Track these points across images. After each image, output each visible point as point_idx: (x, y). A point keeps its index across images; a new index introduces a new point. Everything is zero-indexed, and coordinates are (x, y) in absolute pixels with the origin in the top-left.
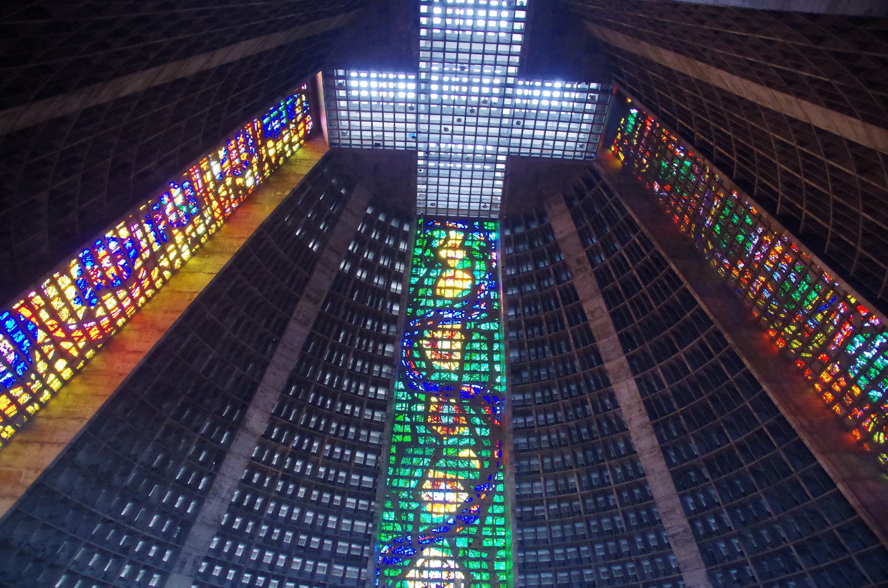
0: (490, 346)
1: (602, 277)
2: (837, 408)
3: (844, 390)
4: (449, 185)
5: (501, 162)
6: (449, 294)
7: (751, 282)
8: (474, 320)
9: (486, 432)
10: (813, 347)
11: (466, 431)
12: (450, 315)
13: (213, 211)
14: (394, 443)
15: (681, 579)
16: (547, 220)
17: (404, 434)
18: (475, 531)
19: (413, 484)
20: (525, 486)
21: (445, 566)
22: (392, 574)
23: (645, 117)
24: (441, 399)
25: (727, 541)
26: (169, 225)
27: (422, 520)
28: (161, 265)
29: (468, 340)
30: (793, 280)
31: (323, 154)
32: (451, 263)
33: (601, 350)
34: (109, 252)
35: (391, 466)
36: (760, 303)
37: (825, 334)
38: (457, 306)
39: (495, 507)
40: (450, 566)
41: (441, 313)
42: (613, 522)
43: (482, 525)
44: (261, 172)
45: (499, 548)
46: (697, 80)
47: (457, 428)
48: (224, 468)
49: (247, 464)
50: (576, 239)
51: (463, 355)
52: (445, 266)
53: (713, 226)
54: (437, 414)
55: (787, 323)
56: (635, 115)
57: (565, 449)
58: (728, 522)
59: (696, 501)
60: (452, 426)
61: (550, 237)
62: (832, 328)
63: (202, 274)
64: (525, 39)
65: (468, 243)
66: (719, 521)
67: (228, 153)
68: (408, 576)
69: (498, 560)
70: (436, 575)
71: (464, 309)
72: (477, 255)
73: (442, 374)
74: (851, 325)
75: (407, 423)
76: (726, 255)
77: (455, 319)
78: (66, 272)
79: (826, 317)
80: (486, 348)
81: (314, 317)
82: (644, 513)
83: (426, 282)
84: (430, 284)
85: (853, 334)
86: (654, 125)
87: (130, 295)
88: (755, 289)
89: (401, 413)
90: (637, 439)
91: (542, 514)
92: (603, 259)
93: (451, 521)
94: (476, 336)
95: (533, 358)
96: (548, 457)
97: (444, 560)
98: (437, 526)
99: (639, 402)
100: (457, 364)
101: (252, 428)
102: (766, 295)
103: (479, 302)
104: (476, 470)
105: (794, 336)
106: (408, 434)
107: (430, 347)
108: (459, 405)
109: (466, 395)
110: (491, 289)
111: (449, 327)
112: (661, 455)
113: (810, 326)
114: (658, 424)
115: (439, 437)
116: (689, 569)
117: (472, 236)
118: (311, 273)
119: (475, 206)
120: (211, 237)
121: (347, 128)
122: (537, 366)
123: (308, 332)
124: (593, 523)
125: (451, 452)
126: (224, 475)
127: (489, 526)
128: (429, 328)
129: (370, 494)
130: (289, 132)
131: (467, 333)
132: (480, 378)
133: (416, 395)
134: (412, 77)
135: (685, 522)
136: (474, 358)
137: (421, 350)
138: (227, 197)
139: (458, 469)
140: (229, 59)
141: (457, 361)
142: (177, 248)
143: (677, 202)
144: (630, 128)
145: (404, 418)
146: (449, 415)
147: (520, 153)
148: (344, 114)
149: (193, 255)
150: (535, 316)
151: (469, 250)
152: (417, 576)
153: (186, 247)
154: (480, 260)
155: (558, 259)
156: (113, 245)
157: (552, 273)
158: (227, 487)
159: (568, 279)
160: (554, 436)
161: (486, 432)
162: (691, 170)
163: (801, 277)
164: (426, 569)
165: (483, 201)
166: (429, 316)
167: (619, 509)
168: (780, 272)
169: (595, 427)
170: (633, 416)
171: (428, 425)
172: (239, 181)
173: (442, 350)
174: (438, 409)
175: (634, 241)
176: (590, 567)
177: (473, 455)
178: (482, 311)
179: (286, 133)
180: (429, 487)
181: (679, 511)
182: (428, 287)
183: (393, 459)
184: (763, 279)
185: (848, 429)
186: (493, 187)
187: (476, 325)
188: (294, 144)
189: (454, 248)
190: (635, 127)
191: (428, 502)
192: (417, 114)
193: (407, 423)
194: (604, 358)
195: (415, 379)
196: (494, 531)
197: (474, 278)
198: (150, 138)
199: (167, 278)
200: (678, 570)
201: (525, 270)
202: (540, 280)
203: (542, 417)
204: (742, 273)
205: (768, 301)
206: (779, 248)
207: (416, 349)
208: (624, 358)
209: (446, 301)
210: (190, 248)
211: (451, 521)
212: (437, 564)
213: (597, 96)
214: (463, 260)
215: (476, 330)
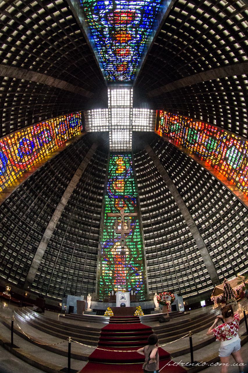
3: (228, 169)
6: (120, 172)
7: (199, 149)
9: (132, 208)
11: (127, 209)
12: (120, 177)
19: (112, 224)
26: (43, 141)
28: (40, 152)
29: (126, 183)
30: (210, 143)
32: (120, 165)
34: (27, 143)
35: (105, 219)
38: (122, 175)
43: (133, 235)
44: (69, 136)
45: (139, 241)
48: (54, 214)
51: (124, 188)
52: (118, 165)
53: (187, 137)
55: (210, 156)
60: (123, 207)
62: (222, 151)
67: (60, 127)
68: (112, 250)
69: (138, 245)
75: (109, 207)
76: (192, 144)
79: (220, 149)
81: (81, 174)
83: (113, 170)
86: (168, 119)
87: (31, 158)
89: (107, 204)
102: (204, 150)
103: (129, 173)
105: (213, 159)
106: (109, 210)
108: (124, 201)
109: (126, 198)
110: (131, 171)
118: (81, 162)
119: (125, 148)
120: (54, 149)
128: (114, 181)
129: (98, 227)
131: (126, 182)
134: (107, 110)
135: (193, 221)
136: (127, 188)
137: (113, 187)
138: (59, 140)
142: (45, 149)
144: (162, 122)
146: (121, 204)
149: (49, 153)
151: (125, 161)
153: (47, 150)
154: (128, 164)
156: (28, 142)
158: (56, 219)
161: (132, 208)
162: (179, 125)
163: (211, 141)
171: (115, 207)
172: (63, 136)
173: (118, 187)
178: (129, 176)
182: (114, 171)
183: (105, 217)
184: (202, 146)
185: (230, 180)
188: (78, 132)
189: (120, 161)
190: (163, 122)
196: (137, 236)
205: (205, 152)
206: (204, 136)
208: (170, 179)
210: (49, 150)
214: (123, 164)
215: (128, 181)
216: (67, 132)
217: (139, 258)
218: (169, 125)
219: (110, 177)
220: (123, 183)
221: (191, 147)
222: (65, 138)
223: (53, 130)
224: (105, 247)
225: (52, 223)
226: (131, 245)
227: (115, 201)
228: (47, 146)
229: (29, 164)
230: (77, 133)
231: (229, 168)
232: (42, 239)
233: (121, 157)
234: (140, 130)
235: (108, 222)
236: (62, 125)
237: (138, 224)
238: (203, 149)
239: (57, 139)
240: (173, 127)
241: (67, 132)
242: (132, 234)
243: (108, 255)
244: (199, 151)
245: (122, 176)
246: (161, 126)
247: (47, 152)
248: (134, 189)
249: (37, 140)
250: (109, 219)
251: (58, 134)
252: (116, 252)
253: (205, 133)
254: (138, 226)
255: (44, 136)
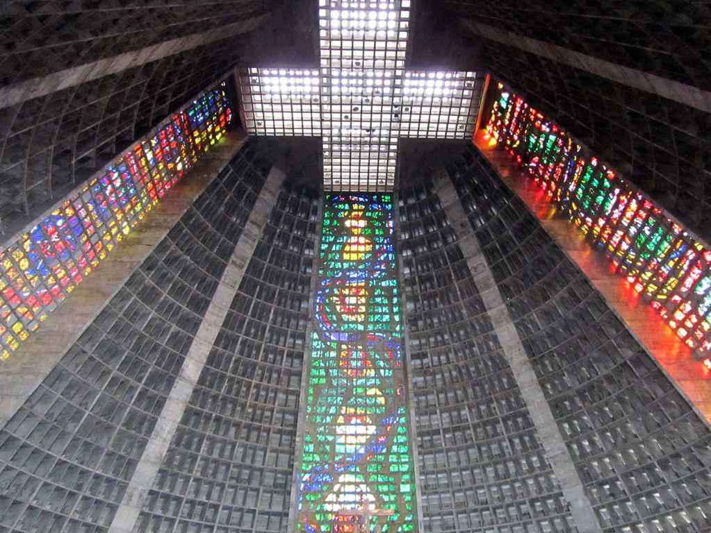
0: (390, 300)
1: (482, 237)
2: (690, 343)
3: (696, 326)
4: (350, 165)
5: (394, 144)
6: (354, 257)
7: (611, 236)
8: (376, 278)
9: (388, 373)
10: (668, 290)
11: (372, 373)
13: (149, 192)
14: (311, 385)
15: (561, 494)
16: (434, 192)
17: (319, 377)
18: (383, 459)
19: (329, 419)
20: (424, 418)
21: (358, 490)
22: (313, 499)
23: (515, 100)
24: (350, 346)
25: (600, 460)
27: (337, 451)
29: (371, 296)
30: (648, 233)
31: (242, 142)
32: (355, 231)
33: (484, 299)
34: (57, 228)
36: (620, 254)
37: (676, 278)
39: (399, 437)
40: (362, 491)
41: (348, 274)
42: (501, 448)
43: (389, 452)
45: (404, 473)
46: (558, 63)
47: (365, 370)
48: (164, 412)
49: (185, 408)
50: (460, 207)
52: (350, 234)
53: (576, 190)
54: (348, 359)
55: (643, 270)
56: (506, 100)
57: (457, 386)
58: (600, 444)
59: (572, 426)
60: (361, 369)
61: (437, 206)
62: (682, 272)
63: (141, 246)
64: (409, 36)
65: (368, 214)
66: (592, 443)
67: (160, 142)
68: (327, 500)
69: (403, 483)
70: (351, 498)
71: (367, 270)
72: (377, 224)
73: (350, 325)
74: (699, 268)
75: (321, 368)
76: (588, 214)
77: (359, 278)
78: (20, 245)
79: (677, 263)
80: (387, 302)
82: (527, 438)
83: (334, 249)
84: (337, 249)
85: (701, 277)
86: (522, 106)
88: (615, 243)
89: (316, 359)
90: (518, 374)
91: (439, 442)
92: (483, 223)
93: (362, 451)
94: (378, 292)
95: (427, 309)
96: (442, 392)
97: (357, 484)
98: (350, 455)
99: (518, 343)
100: (363, 316)
101: (188, 377)
102: (625, 246)
103: (381, 263)
104: (382, 406)
105: (650, 281)
106: (323, 377)
107: (339, 303)
111: (354, 285)
112: (539, 387)
113: (663, 272)
114: (535, 360)
115: (349, 378)
116: (569, 485)
117: (372, 208)
118: (235, 243)
119: (373, 182)
121: (262, 118)
122: (429, 315)
123: (234, 293)
124: (484, 449)
125: (360, 390)
126: (164, 418)
127: (394, 454)
128: (337, 287)
130: (212, 123)
132: (383, 328)
133: (328, 343)
134: (316, 73)
135: (563, 445)
136: (376, 310)
137: (332, 305)
138: (161, 179)
139: (366, 406)
140: (153, 58)
141: (363, 313)
143: (545, 171)
145: (319, 363)
146: (357, 359)
147: (409, 135)
148: (258, 106)
149: (132, 230)
150: (426, 273)
151: (369, 219)
152: (335, 501)
153: (125, 224)
155: (444, 225)
157: (440, 236)
158: (168, 429)
159: (454, 241)
160: (447, 375)
161: (388, 373)
162: (555, 143)
163: (654, 230)
164: (341, 493)
165: (379, 177)
166: (337, 276)
167: (506, 435)
168: (636, 225)
169: (481, 366)
170: (513, 355)
171: (338, 368)
172: (170, 166)
173: (349, 305)
174: (347, 355)
175: (508, 206)
176: (482, 487)
177: (380, 393)
178: (383, 271)
179: (209, 125)
180: (342, 422)
181: (558, 435)
182: (336, 252)
183: (311, 398)
186: (388, 166)
187: (377, 283)
188: (217, 133)
189: (357, 218)
191: (341, 435)
192: (321, 105)
193: (321, 368)
194: (486, 307)
195: (327, 331)
196: (399, 458)
197: (374, 243)
198: (88, 128)
199: (110, 249)
200: (559, 487)
201: (417, 234)
202: (430, 243)
203: (435, 359)
204: (603, 229)
205: (627, 252)
206: (634, 205)
207: (327, 304)
208: (503, 306)
209: (351, 264)
211: (362, 451)
212: (352, 488)
213: (473, 83)
214: (364, 228)
216: (183, 147)
217: (405, 526)
218: (524, 128)
219: (325, 273)
220: (362, 292)
221: (584, 222)
222: (180, 167)
223: (137, 161)
224: (308, 490)
225: (156, 442)
226: (381, 484)
227: (339, 350)
228: (123, 212)
229: (72, 281)
230: (214, 137)
231: (702, 327)
232: (126, 496)
233: (359, 203)
234: (423, 134)
235: (319, 414)
236: (166, 131)
237: (403, 420)
238: (620, 242)
239: (154, 183)
240: (537, 141)
241: (183, 147)
242: (384, 451)
243: (318, 512)
244: (608, 243)
245: (361, 270)
246: (497, 119)
247: (126, 231)
248: (396, 313)
249: (91, 207)
250: (321, 406)
251: (156, 165)
252: (340, 503)
253: (637, 199)
254: (402, 425)
255: (110, 187)
